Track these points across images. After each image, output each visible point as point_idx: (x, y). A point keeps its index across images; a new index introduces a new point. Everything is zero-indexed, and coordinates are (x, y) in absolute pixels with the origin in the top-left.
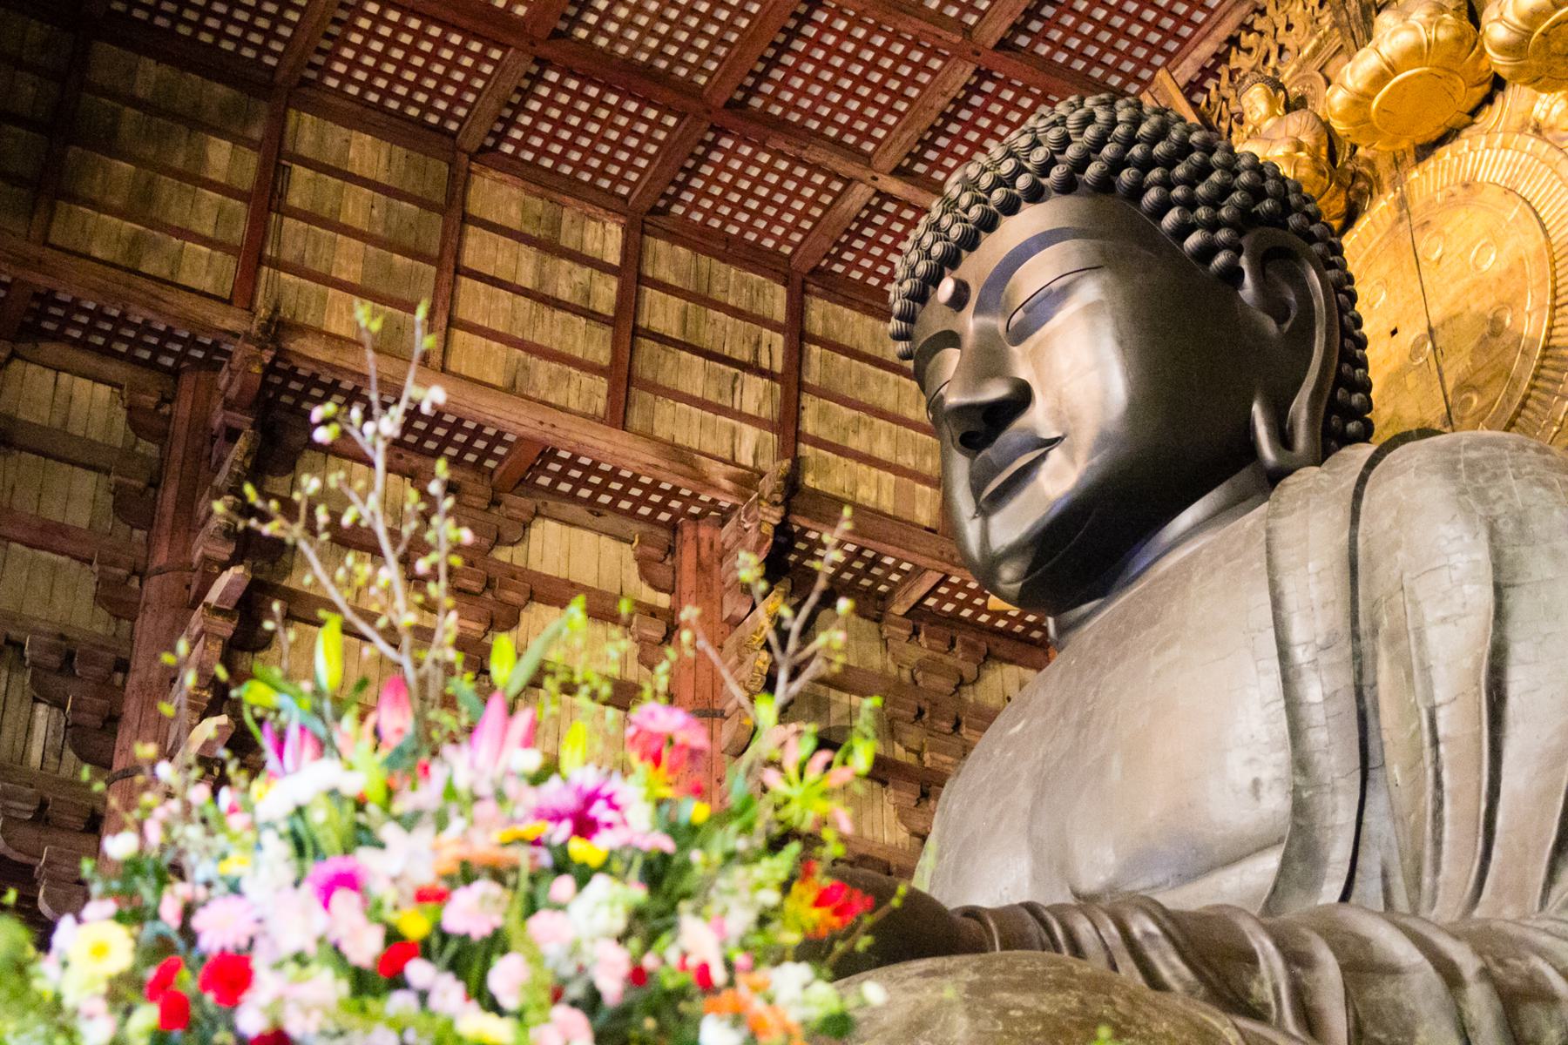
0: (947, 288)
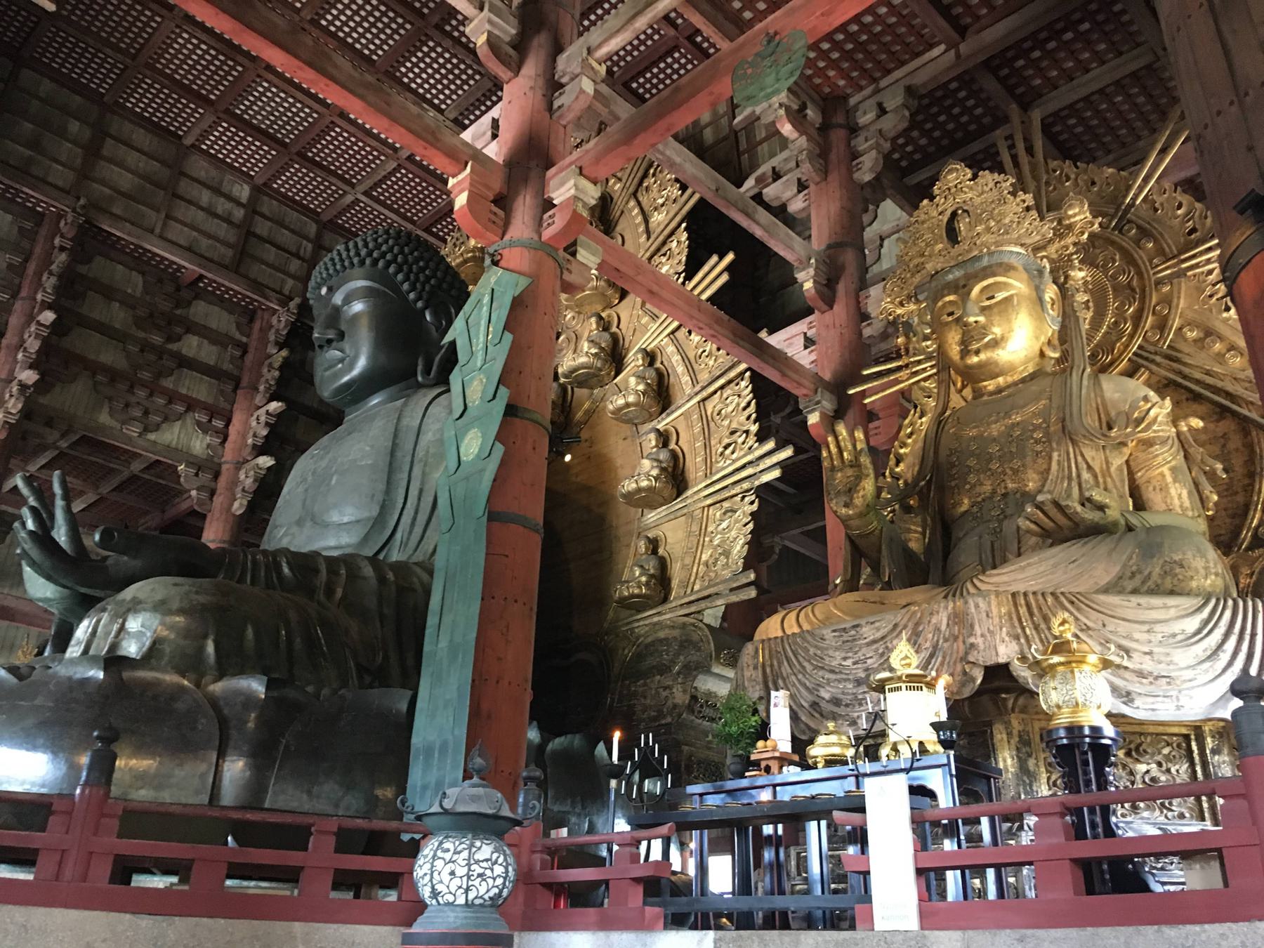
0: (324, 291)
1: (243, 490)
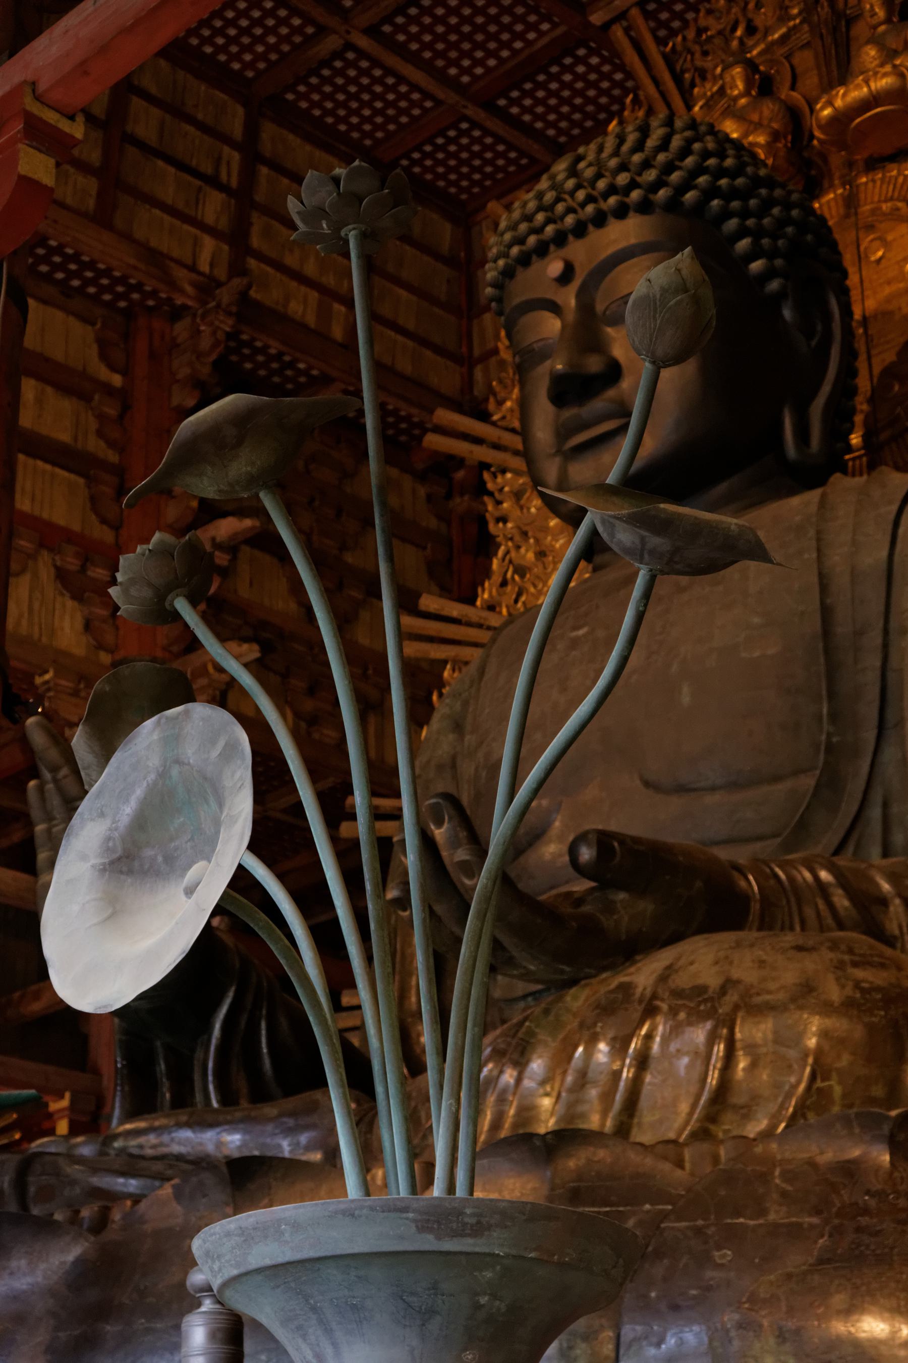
0: (555, 268)
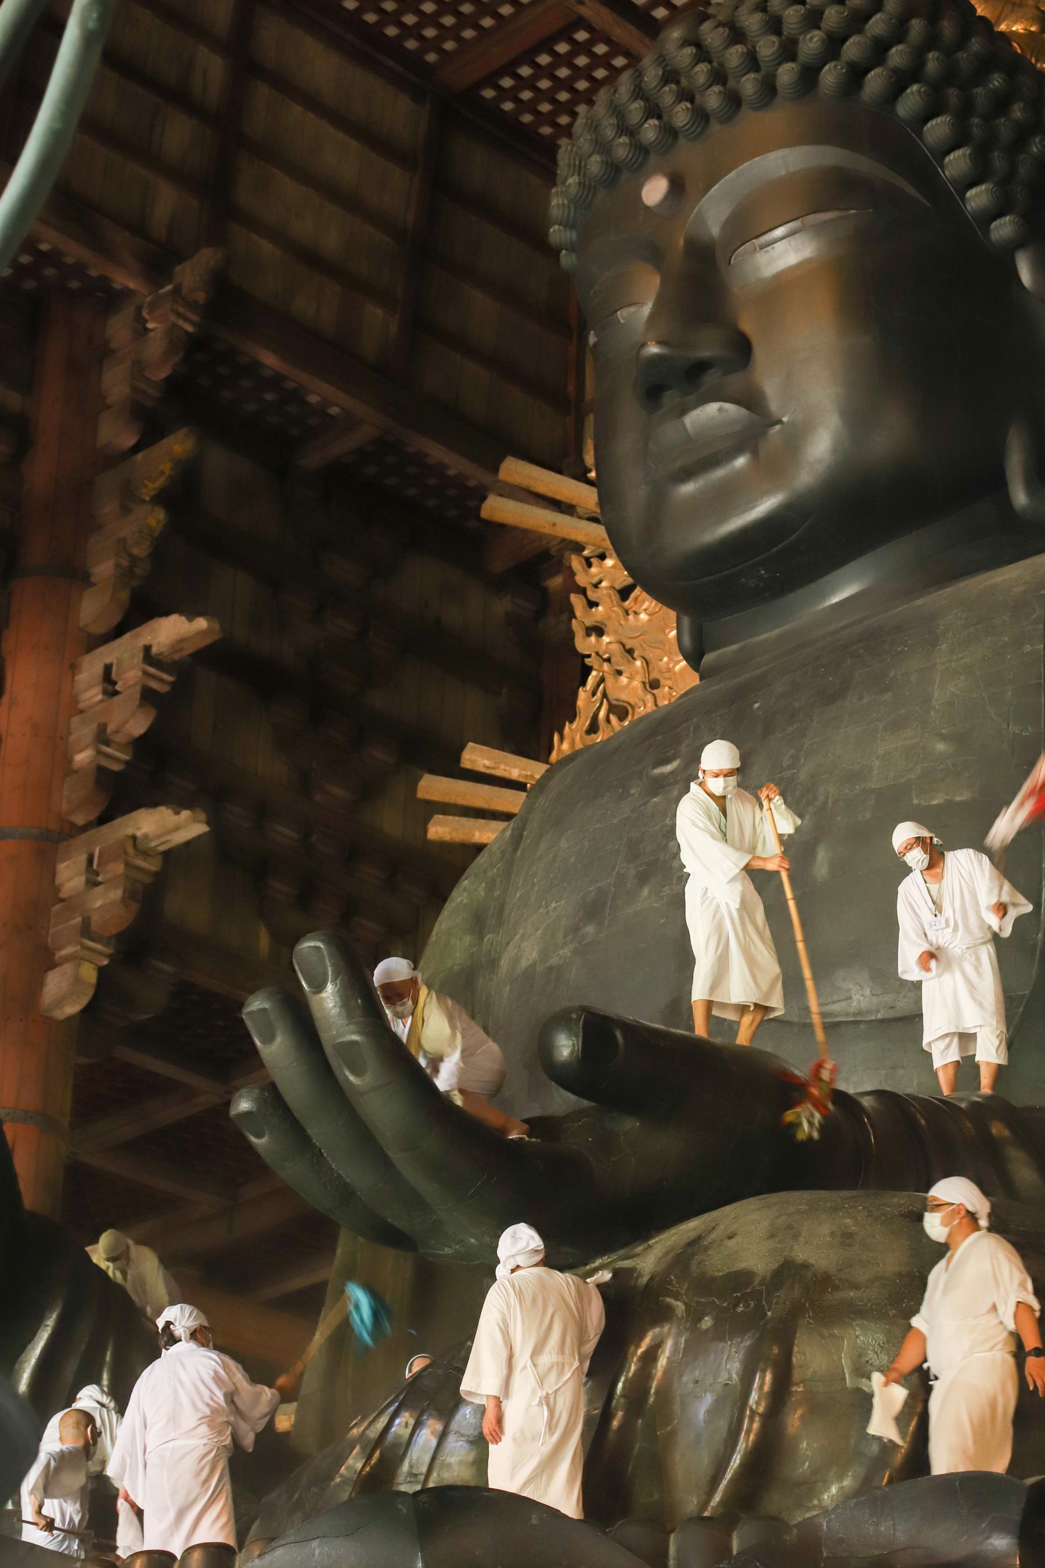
0: (654, 191)
1: (86, 930)
